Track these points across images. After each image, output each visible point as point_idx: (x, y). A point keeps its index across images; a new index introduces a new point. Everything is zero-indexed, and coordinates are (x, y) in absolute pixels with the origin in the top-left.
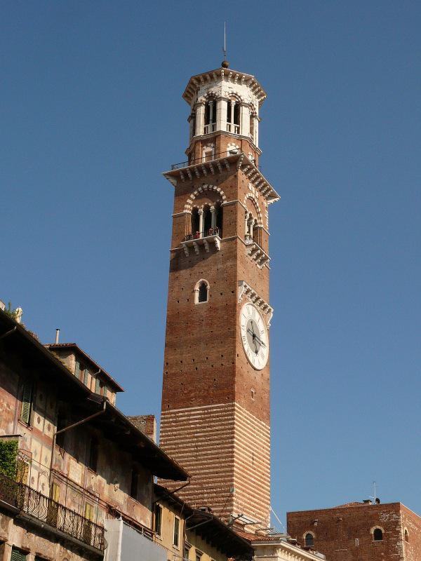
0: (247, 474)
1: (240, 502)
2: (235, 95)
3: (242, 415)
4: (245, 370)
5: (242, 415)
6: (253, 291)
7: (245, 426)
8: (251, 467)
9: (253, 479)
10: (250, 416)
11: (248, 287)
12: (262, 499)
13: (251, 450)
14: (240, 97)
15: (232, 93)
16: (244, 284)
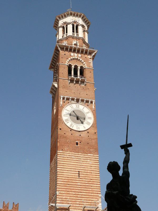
0: (73, 182)
1: (64, 197)
2: (65, 23)
3: (66, 155)
4: (69, 134)
5: (66, 155)
6: (71, 98)
7: (69, 160)
8: (77, 178)
9: (79, 184)
10: (74, 154)
11: (66, 97)
12: (91, 192)
13: (76, 170)
14: (67, 22)
15: (64, 23)
16: (62, 97)
